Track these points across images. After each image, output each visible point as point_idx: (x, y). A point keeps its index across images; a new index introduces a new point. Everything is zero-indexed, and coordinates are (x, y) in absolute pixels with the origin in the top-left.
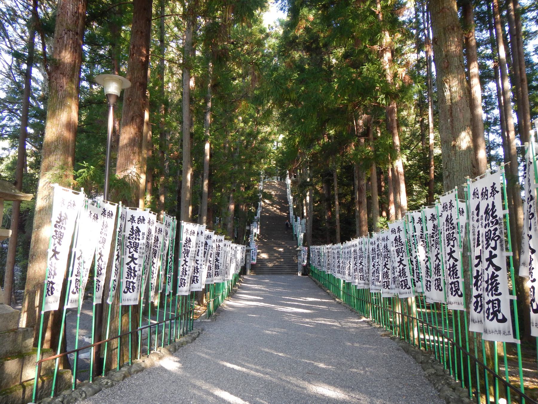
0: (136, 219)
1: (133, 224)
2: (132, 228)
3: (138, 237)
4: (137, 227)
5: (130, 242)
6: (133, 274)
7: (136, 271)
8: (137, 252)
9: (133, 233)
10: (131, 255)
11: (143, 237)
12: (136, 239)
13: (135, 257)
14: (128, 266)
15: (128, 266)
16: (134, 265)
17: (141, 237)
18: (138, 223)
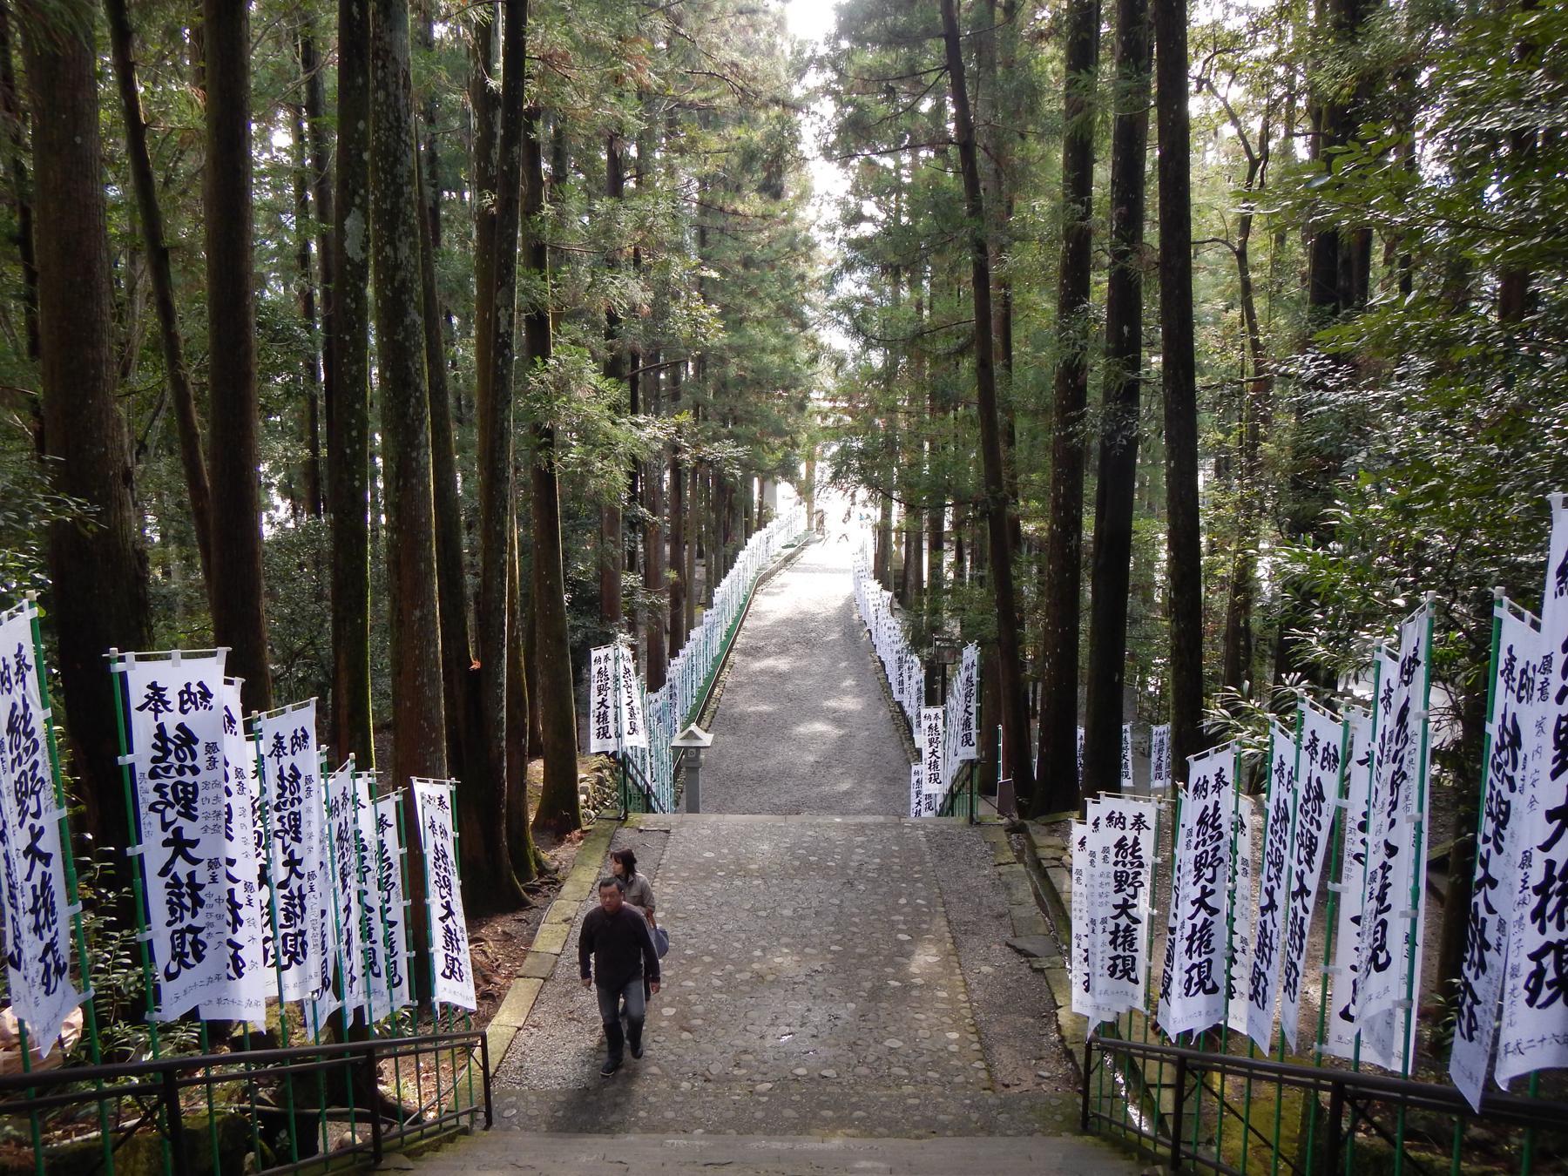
0: (172, 696)
2: (161, 731)
3: (189, 762)
5: (159, 788)
6: (187, 901)
7: (202, 887)
8: (194, 818)
9: (167, 752)
10: (169, 834)
12: (181, 772)
13: (186, 835)
14: (168, 879)
15: (168, 879)
16: (190, 868)
17: (202, 761)
18: (184, 712)
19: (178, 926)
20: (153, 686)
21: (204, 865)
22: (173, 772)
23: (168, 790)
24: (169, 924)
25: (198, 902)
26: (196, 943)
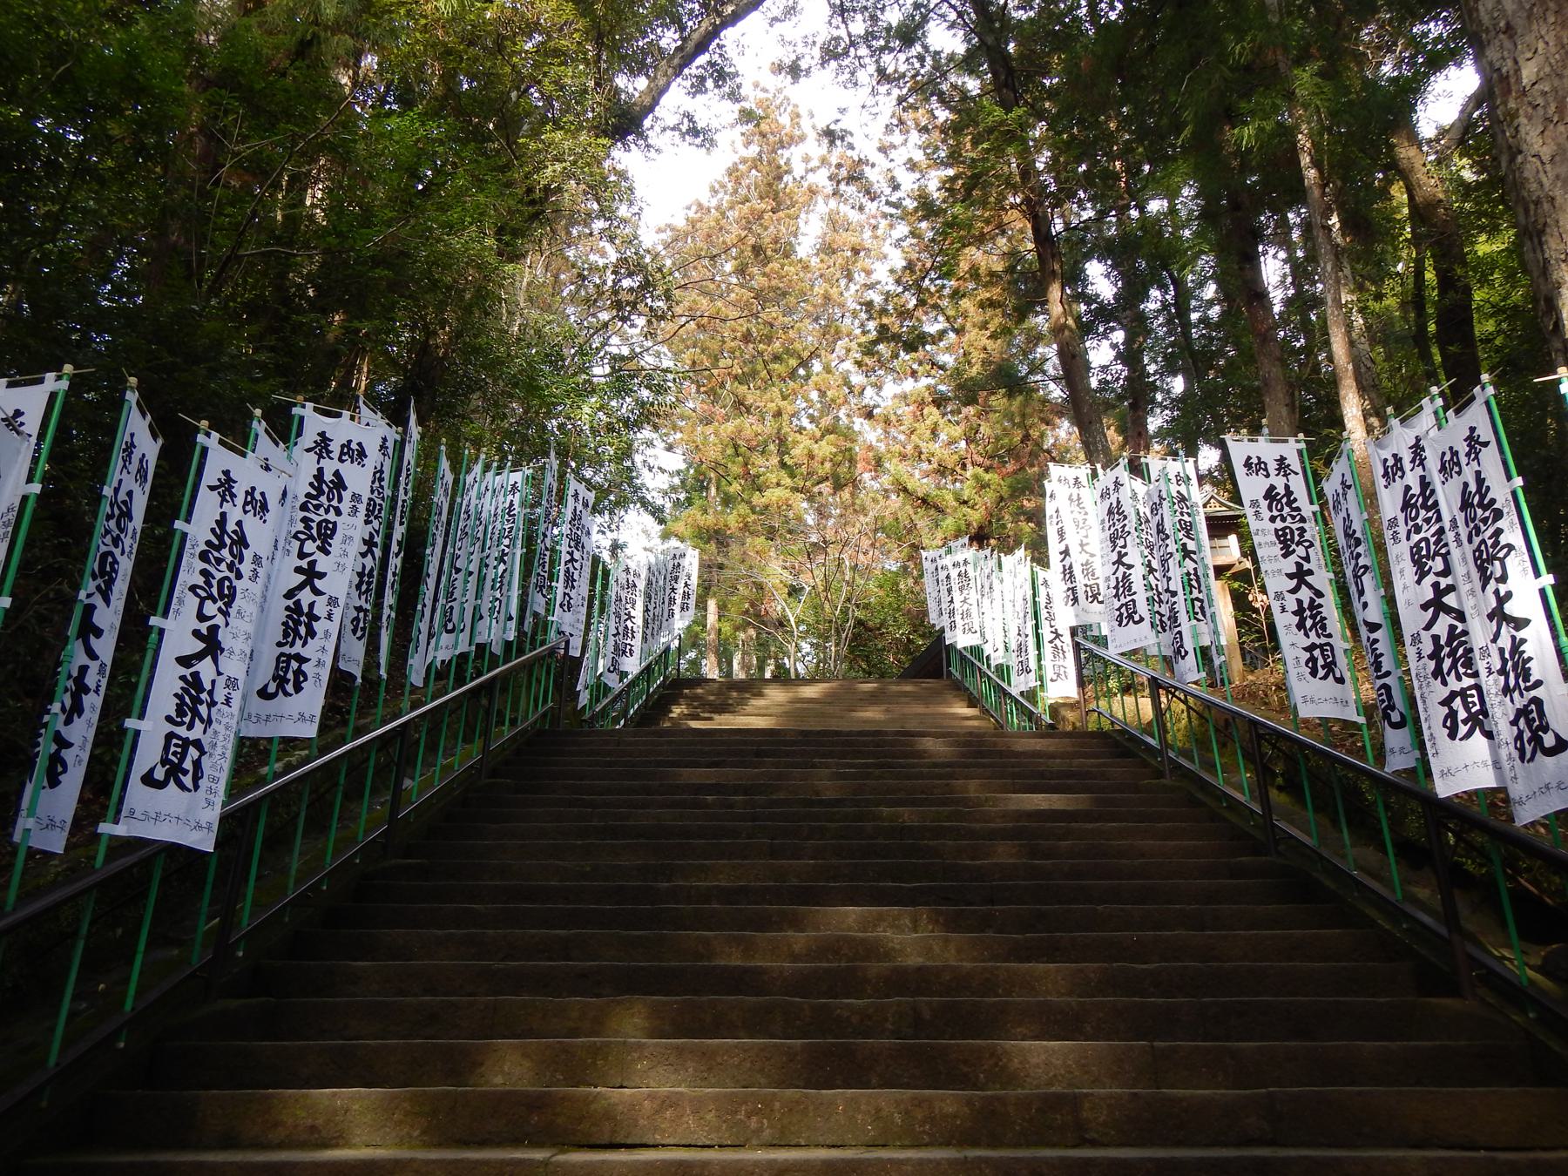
0: (335, 448)
1: (325, 463)
2: (319, 475)
4: (337, 474)
5: (305, 520)
6: (302, 630)
7: (317, 619)
8: (327, 553)
9: (321, 492)
11: (355, 510)
13: (319, 568)
15: (290, 603)
16: (313, 598)
17: (345, 506)
18: (342, 461)
19: (286, 650)
20: (322, 434)
21: (324, 599)
23: (314, 525)
24: (279, 644)
25: (311, 633)
26: (299, 673)
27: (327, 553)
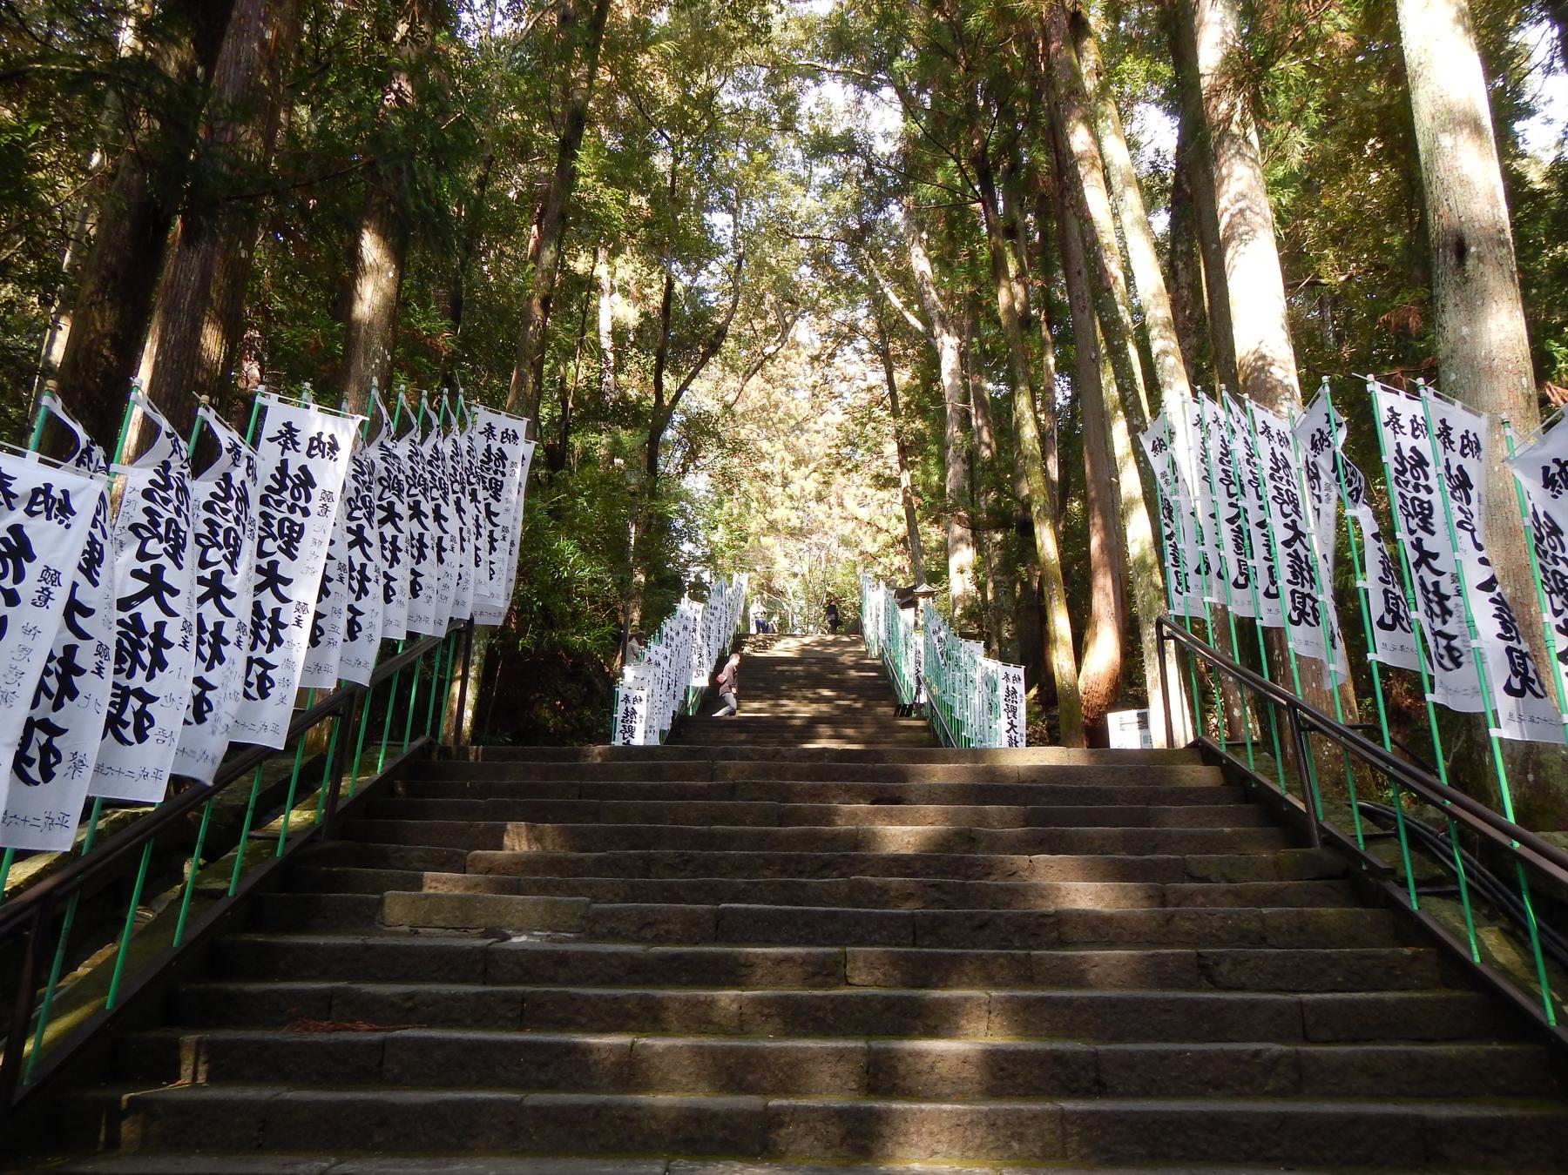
0: (303, 440)
1: (290, 455)
2: (283, 468)
3: (302, 503)
8: (293, 557)
9: (284, 487)
12: (292, 509)
13: (281, 571)
16: (276, 603)
17: (314, 506)
18: (310, 455)
22: (284, 508)
23: (275, 523)
27: (293, 557)
